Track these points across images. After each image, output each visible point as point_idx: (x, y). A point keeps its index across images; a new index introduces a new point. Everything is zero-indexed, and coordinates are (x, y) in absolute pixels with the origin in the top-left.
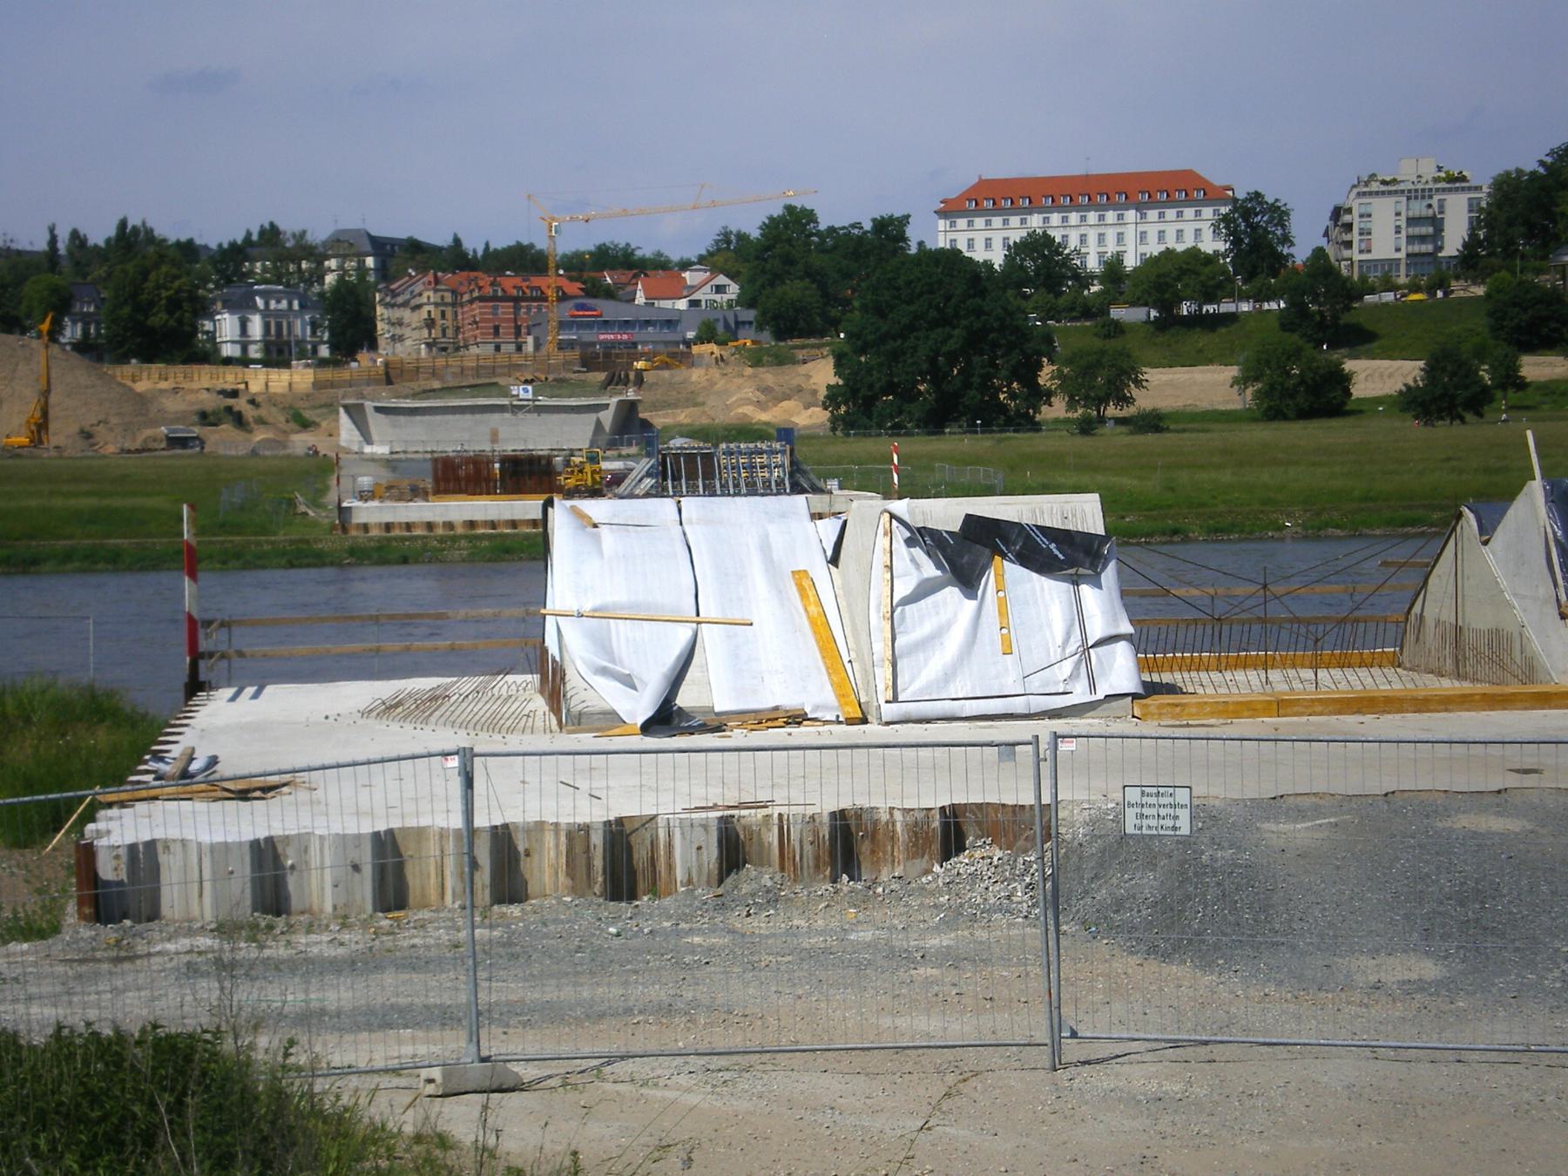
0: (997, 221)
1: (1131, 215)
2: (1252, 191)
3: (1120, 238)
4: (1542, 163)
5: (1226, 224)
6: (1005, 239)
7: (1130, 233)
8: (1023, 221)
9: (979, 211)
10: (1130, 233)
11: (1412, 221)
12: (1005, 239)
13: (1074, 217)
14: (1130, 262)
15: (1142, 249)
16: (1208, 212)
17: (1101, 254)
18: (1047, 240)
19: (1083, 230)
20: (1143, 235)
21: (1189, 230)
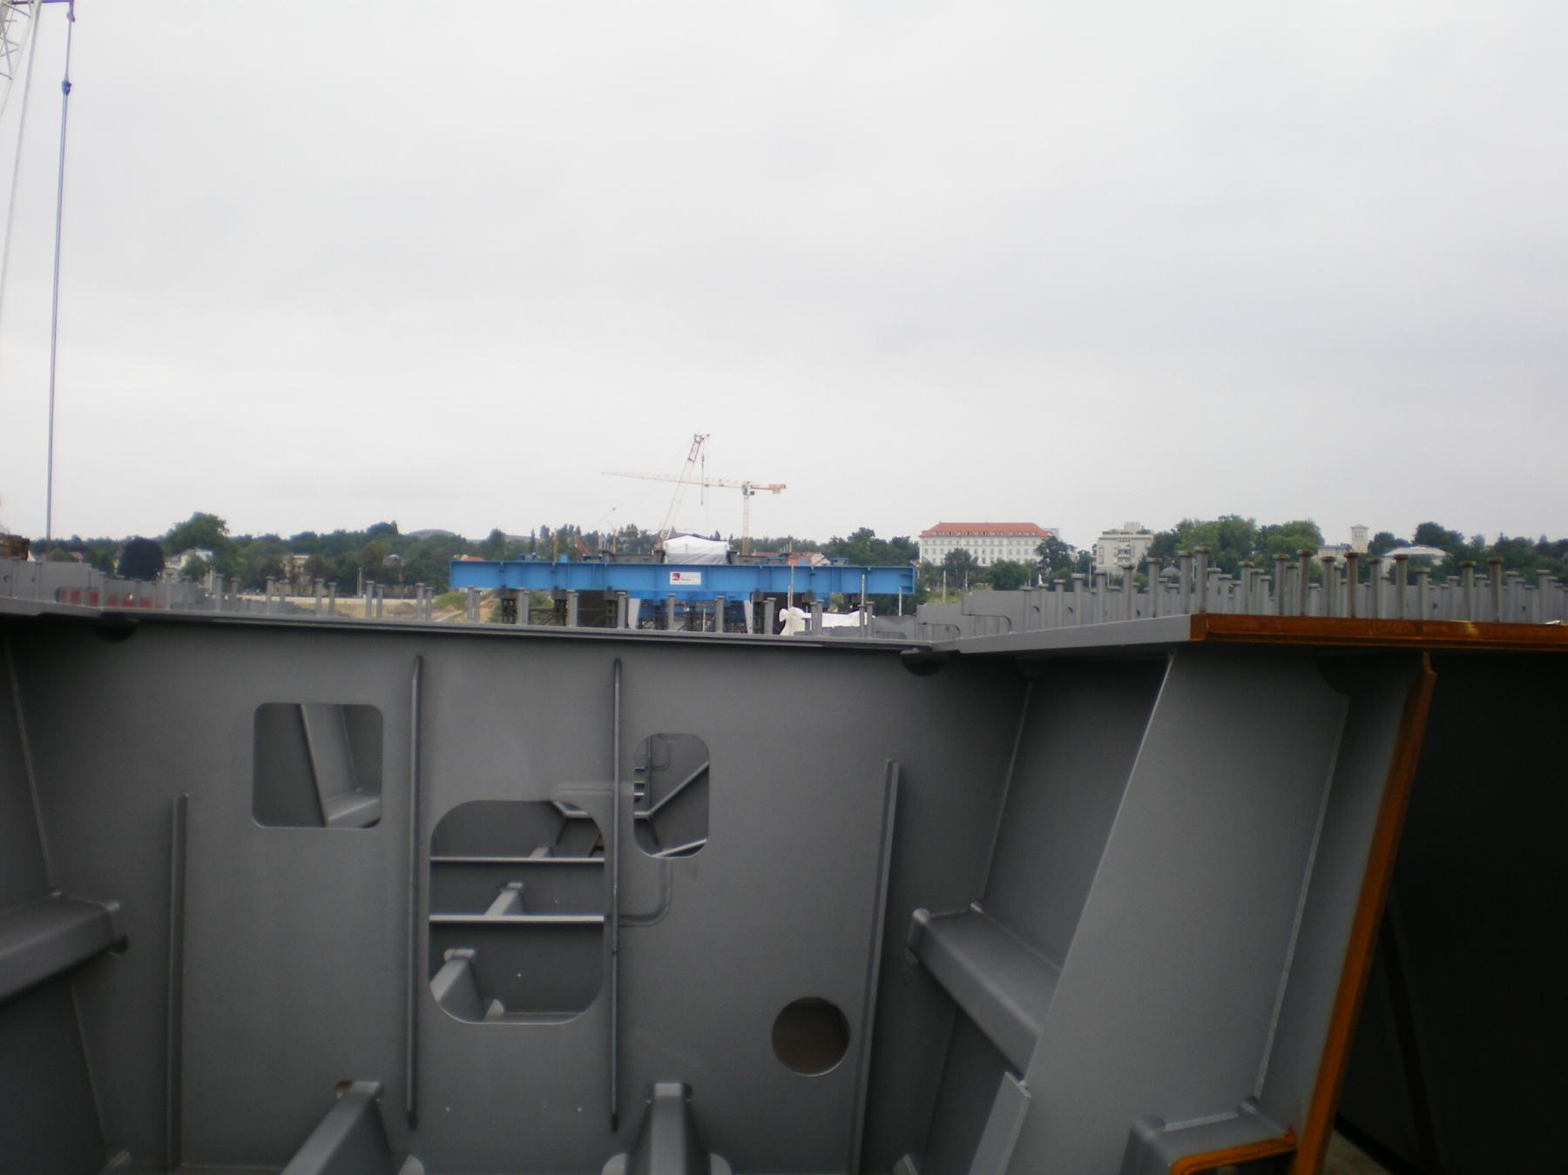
0: (946, 541)
1: (1005, 541)
4: (1172, 530)
5: (1040, 550)
7: (1005, 549)
8: (958, 542)
9: (938, 536)
10: (1005, 549)
11: (1120, 552)
18: (966, 555)
19: (984, 547)
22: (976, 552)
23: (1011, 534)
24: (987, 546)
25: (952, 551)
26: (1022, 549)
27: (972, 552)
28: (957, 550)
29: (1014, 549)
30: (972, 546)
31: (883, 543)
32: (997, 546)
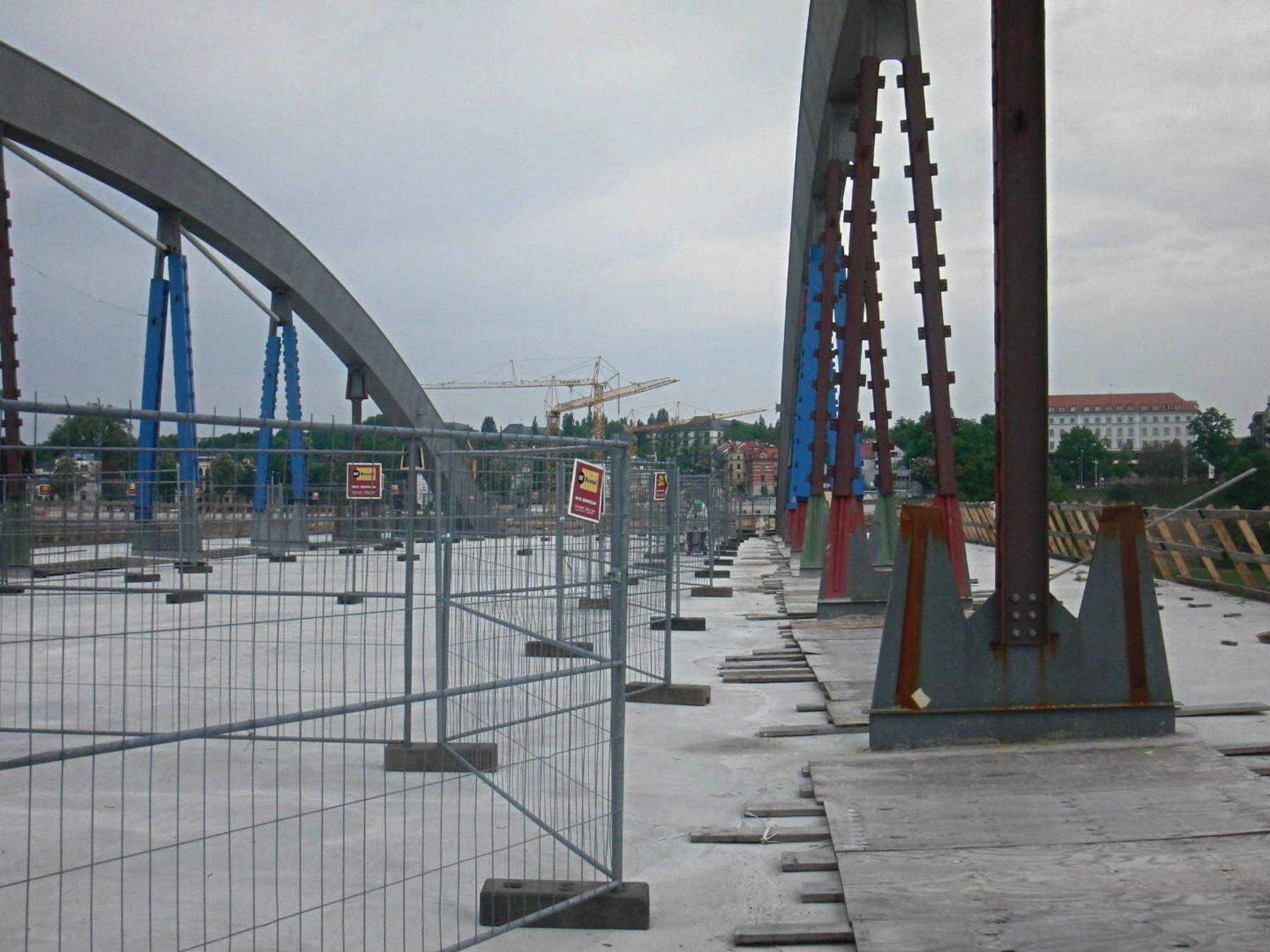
1: (1137, 418)
2: (1209, 407)
3: (1131, 431)
5: (1194, 427)
6: (1062, 431)
7: (1137, 429)
8: (1072, 420)
10: (1137, 429)
12: (1062, 431)
13: (1103, 419)
14: (1138, 446)
15: (1145, 438)
16: (1183, 417)
17: (1120, 442)
18: (1086, 433)
20: (1144, 430)
21: (1172, 427)
22: (1098, 431)
23: (1146, 408)
24: (1113, 424)
25: (1068, 430)
26: (1161, 427)
27: (1094, 433)
28: (1076, 431)
29: (1150, 427)
30: (1103, 425)
31: (968, 424)
32: (1126, 424)
